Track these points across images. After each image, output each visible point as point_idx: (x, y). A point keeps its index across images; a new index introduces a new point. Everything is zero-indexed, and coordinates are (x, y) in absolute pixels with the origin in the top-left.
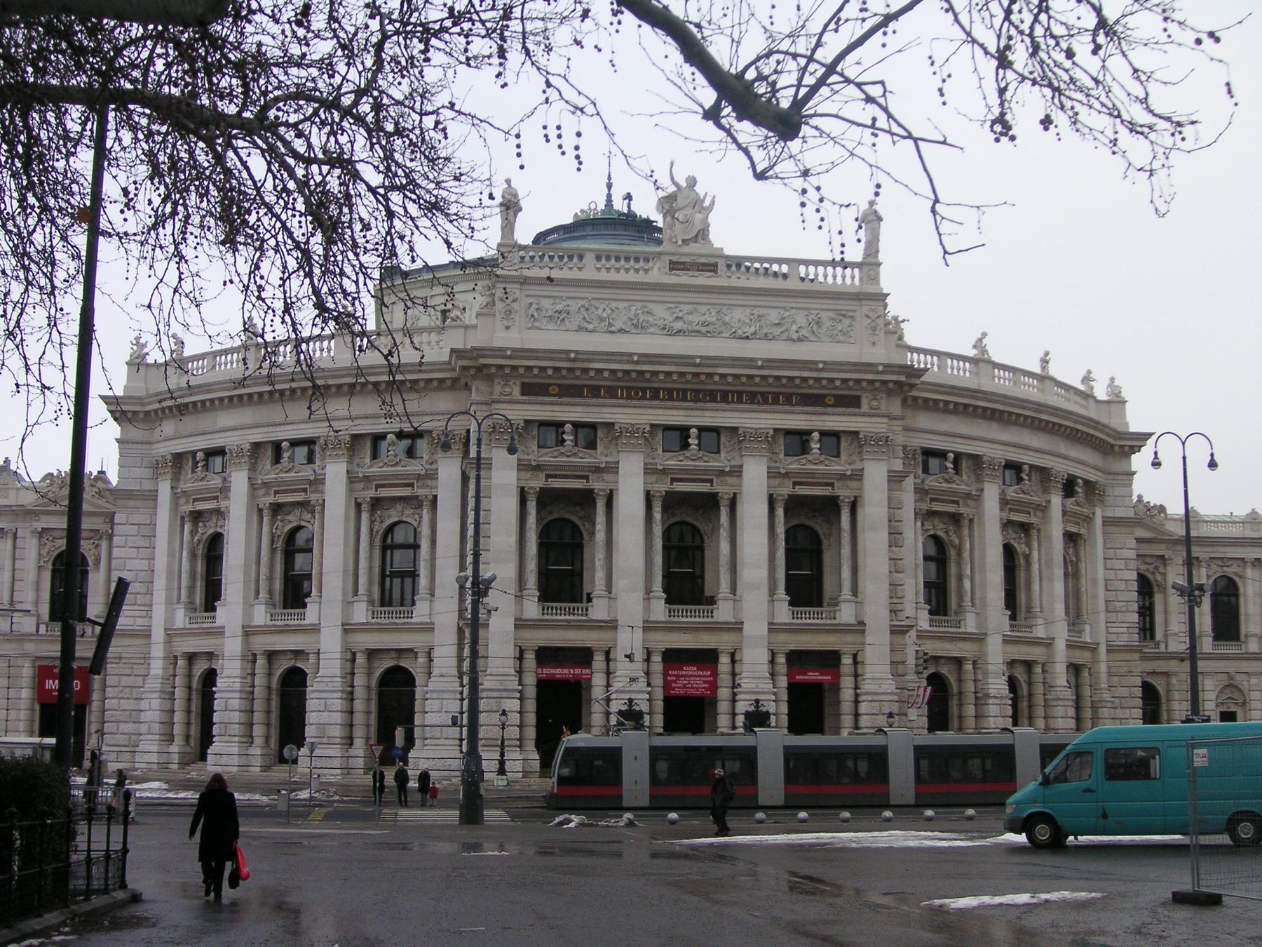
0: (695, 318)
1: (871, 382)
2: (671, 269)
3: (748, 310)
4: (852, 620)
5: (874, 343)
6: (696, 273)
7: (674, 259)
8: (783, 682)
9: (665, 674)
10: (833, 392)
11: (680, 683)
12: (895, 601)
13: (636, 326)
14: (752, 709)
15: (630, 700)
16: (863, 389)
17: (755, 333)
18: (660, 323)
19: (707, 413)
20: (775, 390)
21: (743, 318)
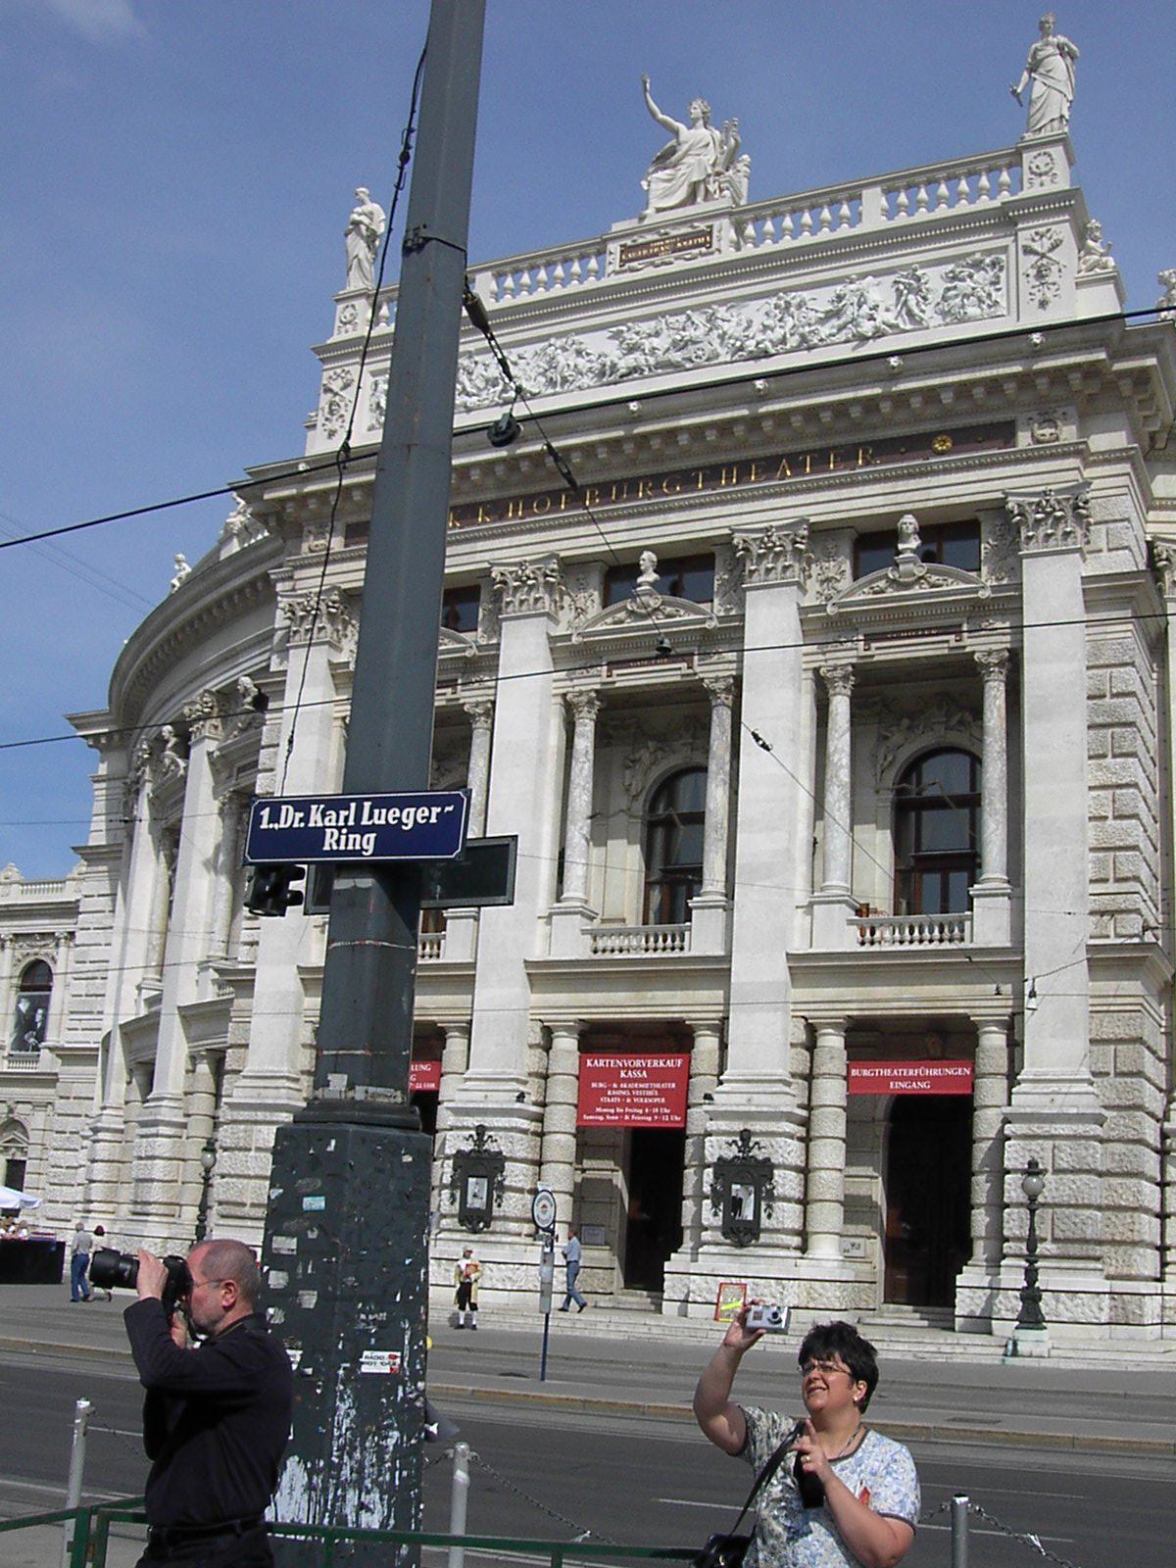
0: (661, 343)
1: (1025, 380)
2: (623, 262)
3: (774, 300)
4: (1003, 940)
5: (1043, 304)
6: (670, 258)
7: (629, 242)
8: (832, 1092)
9: (583, 1077)
10: (949, 424)
11: (614, 1095)
12: (1112, 887)
13: (552, 382)
14: (731, 1153)
15: (481, 1130)
16: (1011, 404)
17: (783, 341)
18: (596, 366)
19: (672, 517)
20: (818, 444)
21: (759, 320)
